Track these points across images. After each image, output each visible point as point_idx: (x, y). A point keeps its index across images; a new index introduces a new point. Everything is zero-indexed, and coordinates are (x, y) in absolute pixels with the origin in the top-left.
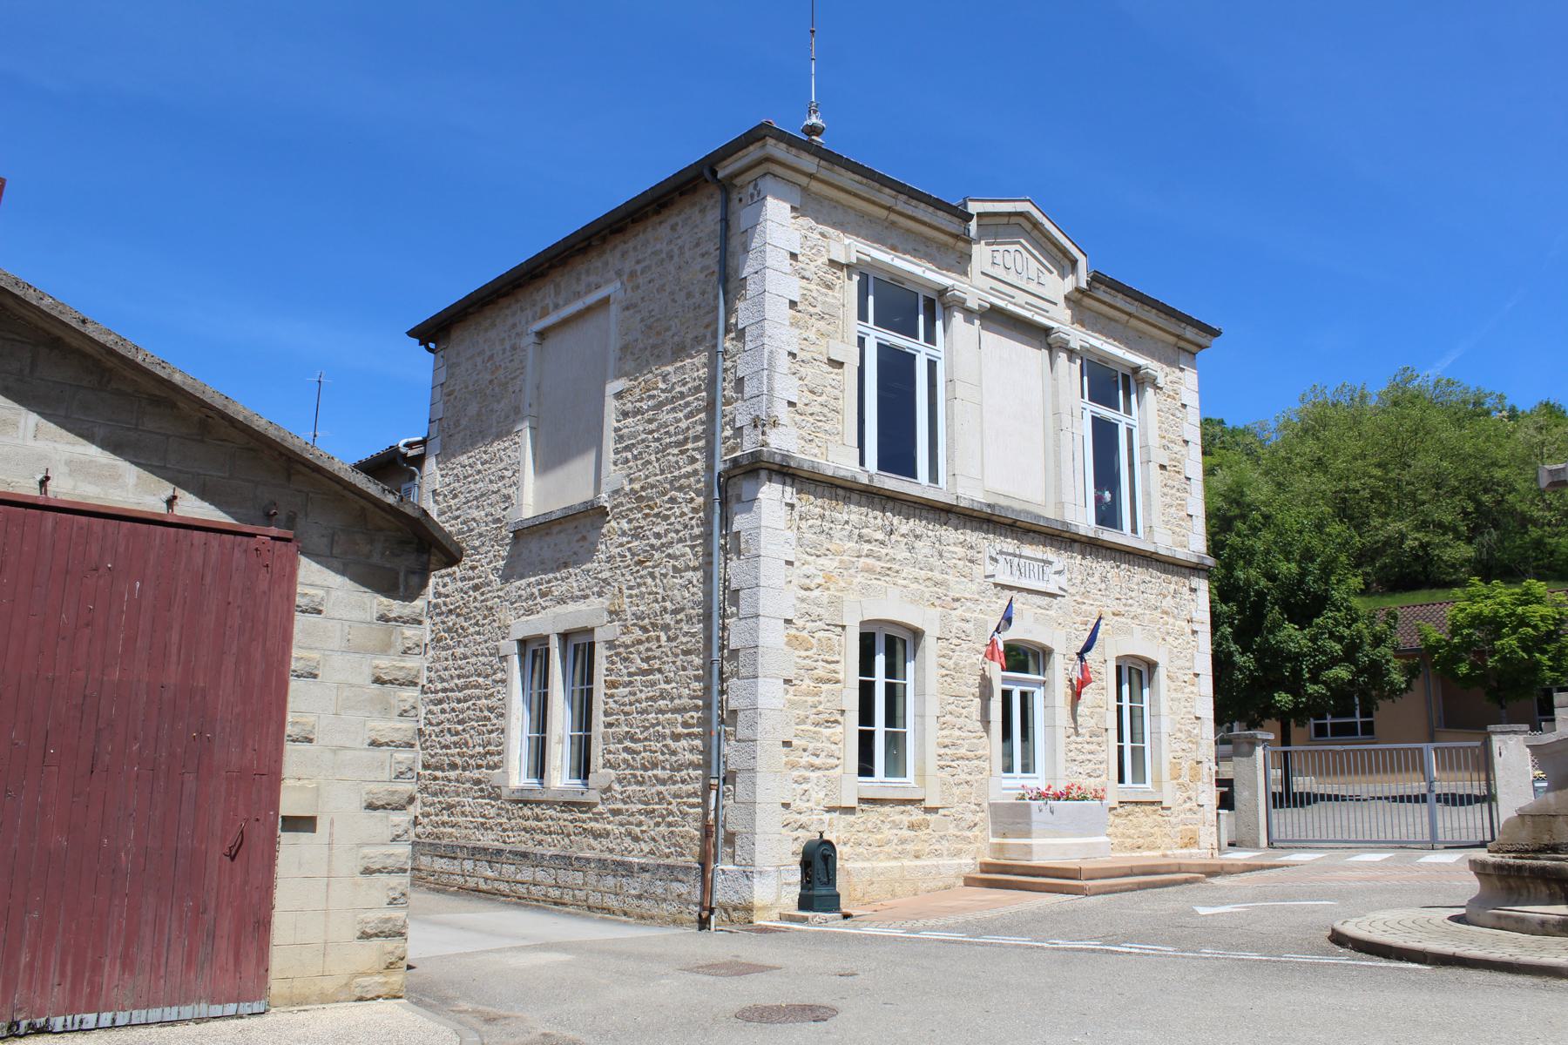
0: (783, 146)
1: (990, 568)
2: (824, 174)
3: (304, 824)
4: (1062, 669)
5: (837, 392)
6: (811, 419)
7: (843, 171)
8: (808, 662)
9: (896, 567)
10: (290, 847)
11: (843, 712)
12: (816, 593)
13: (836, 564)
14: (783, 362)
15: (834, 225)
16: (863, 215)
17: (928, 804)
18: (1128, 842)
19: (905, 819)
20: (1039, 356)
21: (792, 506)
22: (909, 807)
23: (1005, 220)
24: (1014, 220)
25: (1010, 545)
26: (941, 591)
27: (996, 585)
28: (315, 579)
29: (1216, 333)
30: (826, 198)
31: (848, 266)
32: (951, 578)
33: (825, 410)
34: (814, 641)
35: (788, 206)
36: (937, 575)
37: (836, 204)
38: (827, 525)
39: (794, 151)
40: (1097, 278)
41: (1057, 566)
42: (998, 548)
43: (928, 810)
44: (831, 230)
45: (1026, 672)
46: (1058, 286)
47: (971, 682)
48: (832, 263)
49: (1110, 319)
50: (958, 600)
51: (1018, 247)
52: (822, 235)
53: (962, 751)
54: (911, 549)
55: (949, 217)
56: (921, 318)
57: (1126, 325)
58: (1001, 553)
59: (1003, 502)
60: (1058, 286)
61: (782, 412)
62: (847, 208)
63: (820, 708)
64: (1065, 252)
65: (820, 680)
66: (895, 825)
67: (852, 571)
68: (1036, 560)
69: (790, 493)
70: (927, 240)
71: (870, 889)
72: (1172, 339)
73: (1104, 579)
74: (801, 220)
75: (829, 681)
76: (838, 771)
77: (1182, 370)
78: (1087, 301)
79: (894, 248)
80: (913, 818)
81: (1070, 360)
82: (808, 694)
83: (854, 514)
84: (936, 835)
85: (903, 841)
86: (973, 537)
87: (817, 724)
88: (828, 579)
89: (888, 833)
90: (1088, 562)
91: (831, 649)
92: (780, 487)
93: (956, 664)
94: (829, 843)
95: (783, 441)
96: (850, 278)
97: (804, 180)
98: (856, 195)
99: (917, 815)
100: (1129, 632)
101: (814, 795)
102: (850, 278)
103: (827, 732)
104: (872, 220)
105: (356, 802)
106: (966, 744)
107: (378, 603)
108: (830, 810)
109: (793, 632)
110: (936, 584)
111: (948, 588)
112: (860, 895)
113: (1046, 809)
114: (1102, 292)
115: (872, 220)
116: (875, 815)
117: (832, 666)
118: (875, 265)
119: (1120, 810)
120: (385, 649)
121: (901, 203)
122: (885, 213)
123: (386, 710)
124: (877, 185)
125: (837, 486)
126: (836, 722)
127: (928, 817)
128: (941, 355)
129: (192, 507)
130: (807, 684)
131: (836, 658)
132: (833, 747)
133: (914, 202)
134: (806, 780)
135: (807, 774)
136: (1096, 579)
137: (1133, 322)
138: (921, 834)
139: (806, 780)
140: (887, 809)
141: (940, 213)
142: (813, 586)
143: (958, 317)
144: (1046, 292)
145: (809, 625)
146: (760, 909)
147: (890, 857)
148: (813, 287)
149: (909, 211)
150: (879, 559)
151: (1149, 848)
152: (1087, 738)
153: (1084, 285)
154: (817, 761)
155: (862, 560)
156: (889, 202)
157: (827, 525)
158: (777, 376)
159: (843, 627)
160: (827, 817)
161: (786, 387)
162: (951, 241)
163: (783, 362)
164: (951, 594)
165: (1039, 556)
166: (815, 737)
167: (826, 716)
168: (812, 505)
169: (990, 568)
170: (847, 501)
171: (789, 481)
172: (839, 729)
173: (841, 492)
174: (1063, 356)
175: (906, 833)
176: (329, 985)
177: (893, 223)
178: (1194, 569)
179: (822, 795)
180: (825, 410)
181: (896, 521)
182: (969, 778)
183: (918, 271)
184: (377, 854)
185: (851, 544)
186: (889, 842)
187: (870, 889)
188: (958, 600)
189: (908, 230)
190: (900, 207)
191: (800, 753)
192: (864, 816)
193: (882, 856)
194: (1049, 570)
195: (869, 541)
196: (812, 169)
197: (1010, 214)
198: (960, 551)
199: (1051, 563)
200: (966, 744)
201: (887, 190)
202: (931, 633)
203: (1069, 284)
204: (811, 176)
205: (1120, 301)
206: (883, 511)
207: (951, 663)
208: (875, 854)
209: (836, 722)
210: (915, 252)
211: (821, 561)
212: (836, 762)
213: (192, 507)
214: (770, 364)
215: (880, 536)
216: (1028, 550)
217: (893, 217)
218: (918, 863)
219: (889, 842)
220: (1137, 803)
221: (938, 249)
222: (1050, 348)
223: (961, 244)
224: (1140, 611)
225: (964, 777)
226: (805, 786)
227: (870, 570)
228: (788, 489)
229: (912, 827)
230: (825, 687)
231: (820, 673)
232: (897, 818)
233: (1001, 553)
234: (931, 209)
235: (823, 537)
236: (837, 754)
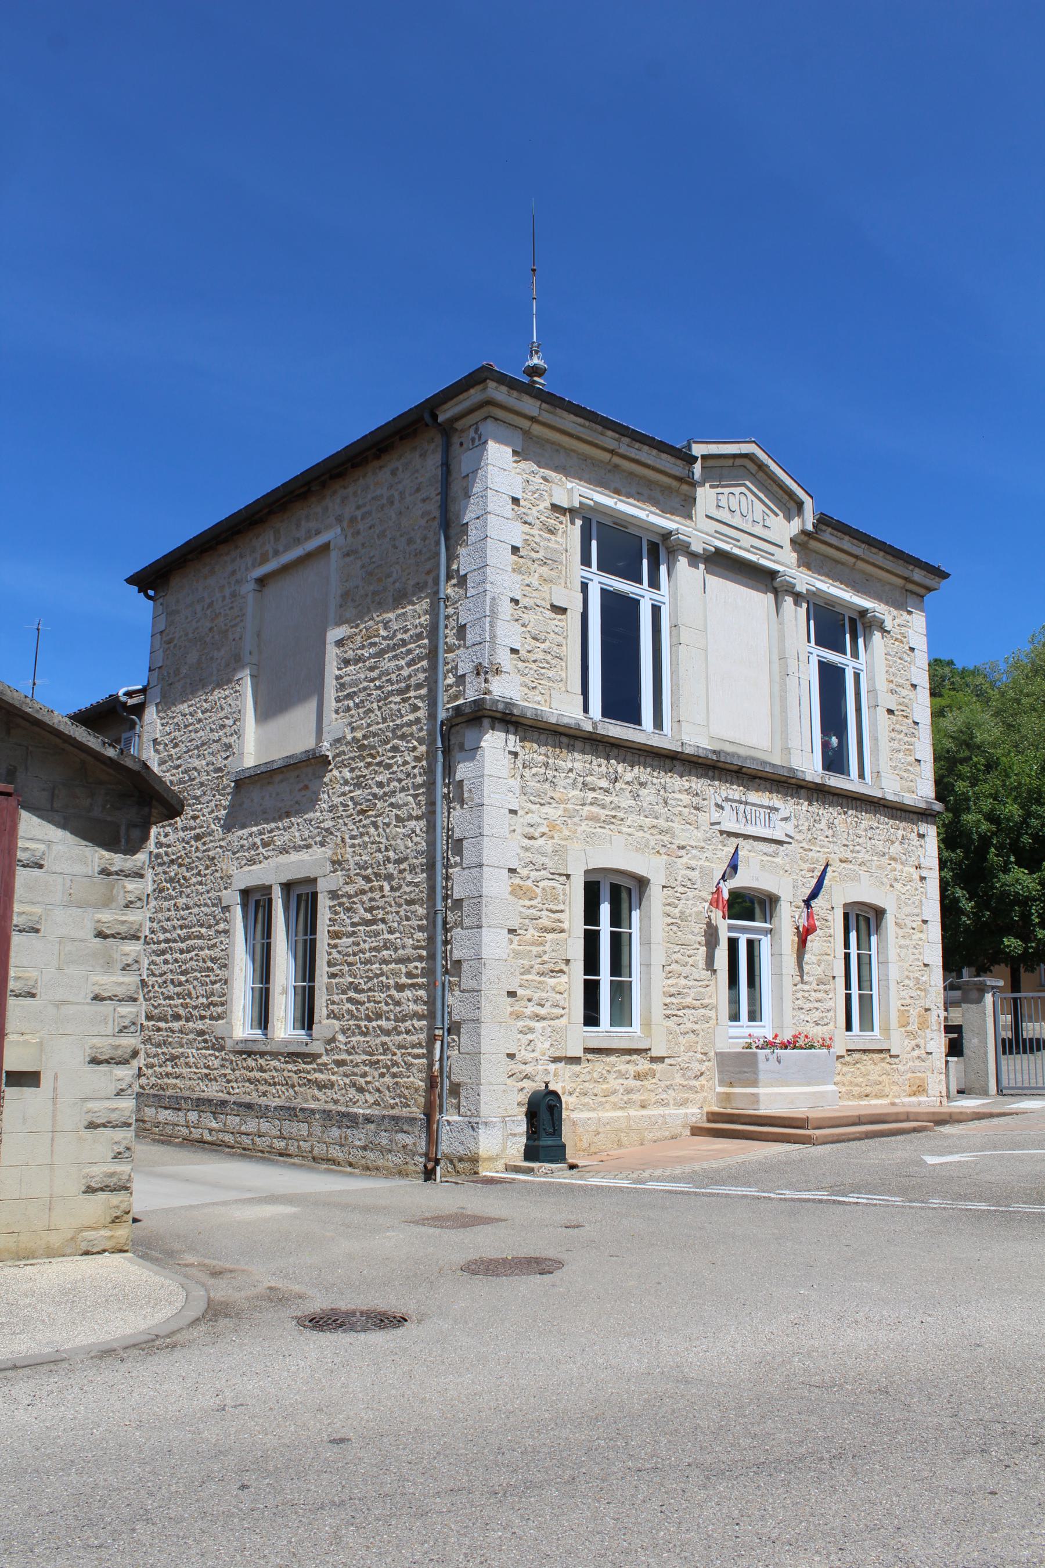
0: (504, 389)
1: (715, 816)
2: (546, 417)
3: (28, 1079)
4: (788, 917)
5: (560, 639)
6: (534, 666)
7: (565, 414)
9: (621, 815)
11: (568, 962)
12: (541, 842)
13: (560, 812)
14: (506, 609)
15: (556, 469)
16: (585, 458)
17: (654, 1053)
18: (856, 1090)
19: (631, 1068)
20: (762, 601)
21: (515, 755)
22: (635, 1057)
23: (730, 462)
25: (735, 792)
26: (666, 839)
27: (722, 832)
28: (34, 832)
29: (944, 575)
30: (548, 441)
31: (571, 510)
32: (676, 826)
33: (549, 657)
34: (538, 891)
35: (510, 450)
36: (662, 823)
37: (558, 447)
38: (550, 773)
39: (515, 394)
40: (823, 521)
41: (784, 813)
42: (724, 794)
43: (654, 1060)
44: (553, 474)
45: (753, 919)
46: (784, 529)
47: (697, 930)
48: (555, 507)
49: (837, 562)
50: (683, 848)
51: (743, 489)
52: (545, 479)
53: (689, 1000)
54: (636, 797)
55: (672, 460)
56: (645, 562)
57: (853, 568)
58: (727, 799)
59: (729, 748)
60: (784, 529)
61: (504, 659)
62: (569, 451)
63: (545, 958)
64: (791, 494)
65: (545, 930)
66: (621, 1075)
67: (576, 820)
68: (763, 807)
69: (513, 741)
70: (650, 483)
71: (595, 1139)
72: (900, 582)
73: (831, 825)
74: (524, 465)
75: (553, 930)
76: (563, 1021)
77: (910, 613)
78: (813, 544)
79: (617, 492)
80: (640, 1068)
81: (797, 603)
82: (533, 944)
83: (578, 761)
84: (663, 1084)
85: (629, 1091)
86: (698, 784)
87: (542, 974)
88: (552, 827)
89: (614, 1083)
90: (815, 808)
91: (556, 898)
92: (503, 735)
93: (682, 912)
94: (555, 1093)
95: (507, 688)
96: (573, 523)
97: (525, 424)
98: (579, 439)
99: (643, 1064)
100: (857, 878)
101: (539, 1045)
102: (573, 523)
103: (552, 982)
104: (595, 463)
105: (78, 1058)
106: (692, 993)
107: (99, 856)
108: (556, 1060)
109: (517, 881)
110: (661, 832)
111: (673, 836)
112: (585, 1145)
113: (773, 1059)
114: (828, 535)
115: (595, 463)
116: (600, 1065)
117: (557, 916)
118: (598, 509)
119: (847, 1059)
120: (107, 903)
121: (624, 446)
122: (606, 456)
123: (108, 964)
124: (600, 428)
125: (561, 734)
126: (561, 971)
127: (654, 1066)
128: (666, 600)
130: (532, 933)
131: (561, 907)
132: (558, 996)
133: (637, 445)
134: (531, 1030)
135: (532, 1024)
136: (823, 825)
137: (861, 565)
139: (531, 1030)
140: (612, 1059)
141: (664, 456)
142: (537, 835)
143: (683, 562)
144: (771, 535)
145: (533, 874)
146: (486, 1159)
147: (616, 1107)
148: (535, 532)
149: (633, 453)
150: (603, 807)
151: (877, 1097)
152: (814, 986)
153: (810, 527)
154: (542, 1011)
155: (587, 808)
156: (612, 444)
157: (550, 773)
158: (499, 623)
159: (568, 876)
160: (552, 1067)
161: (508, 634)
162: (675, 484)
163: (506, 609)
164: (677, 842)
165: (766, 803)
166: (540, 987)
167: (550, 966)
168: (535, 753)
169: (715, 816)
170: (571, 748)
171: (512, 729)
172: (564, 978)
173: (565, 740)
174: (789, 600)
175: (632, 1083)
176: (55, 1240)
177: (616, 466)
179: (547, 1045)
180: (549, 657)
181: (620, 768)
182: (695, 1027)
183: (642, 514)
184: (100, 1109)
185: (576, 792)
186: (615, 1092)
187: (595, 1139)
188: (683, 848)
190: (623, 449)
191: (525, 1003)
192: (590, 1064)
193: (607, 1106)
194: (776, 817)
195: (593, 789)
196: (534, 412)
197: (735, 456)
198: (685, 798)
199: (777, 810)
200: (692, 993)
201: (610, 433)
202: (657, 880)
203: (794, 527)
204: (533, 419)
205: (847, 543)
207: (676, 912)
208: (601, 1104)
209: (561, 971)
210: (639, 496)
211: (546, 809)
212: (562, 1012)
214: (492, 611)
215: (604, 783)
216: (754, 797)
217: (616, 460)
218: (644, 1112)
219: (615, 1092)
220: (864, 1051)
221: (662, 492)
222: (776, 592)
224: (867, 857)
225: (690, 1026)
226: (530, 1037)
227: (595, 818)
228: (511, 737)
229: (638, 1076)
230: (550, 936)
231: (545, 922)
232: (623, 1067)
233: (727, 799)
234: (655, 452)
235: (547, 785)
236: (561, 1004)
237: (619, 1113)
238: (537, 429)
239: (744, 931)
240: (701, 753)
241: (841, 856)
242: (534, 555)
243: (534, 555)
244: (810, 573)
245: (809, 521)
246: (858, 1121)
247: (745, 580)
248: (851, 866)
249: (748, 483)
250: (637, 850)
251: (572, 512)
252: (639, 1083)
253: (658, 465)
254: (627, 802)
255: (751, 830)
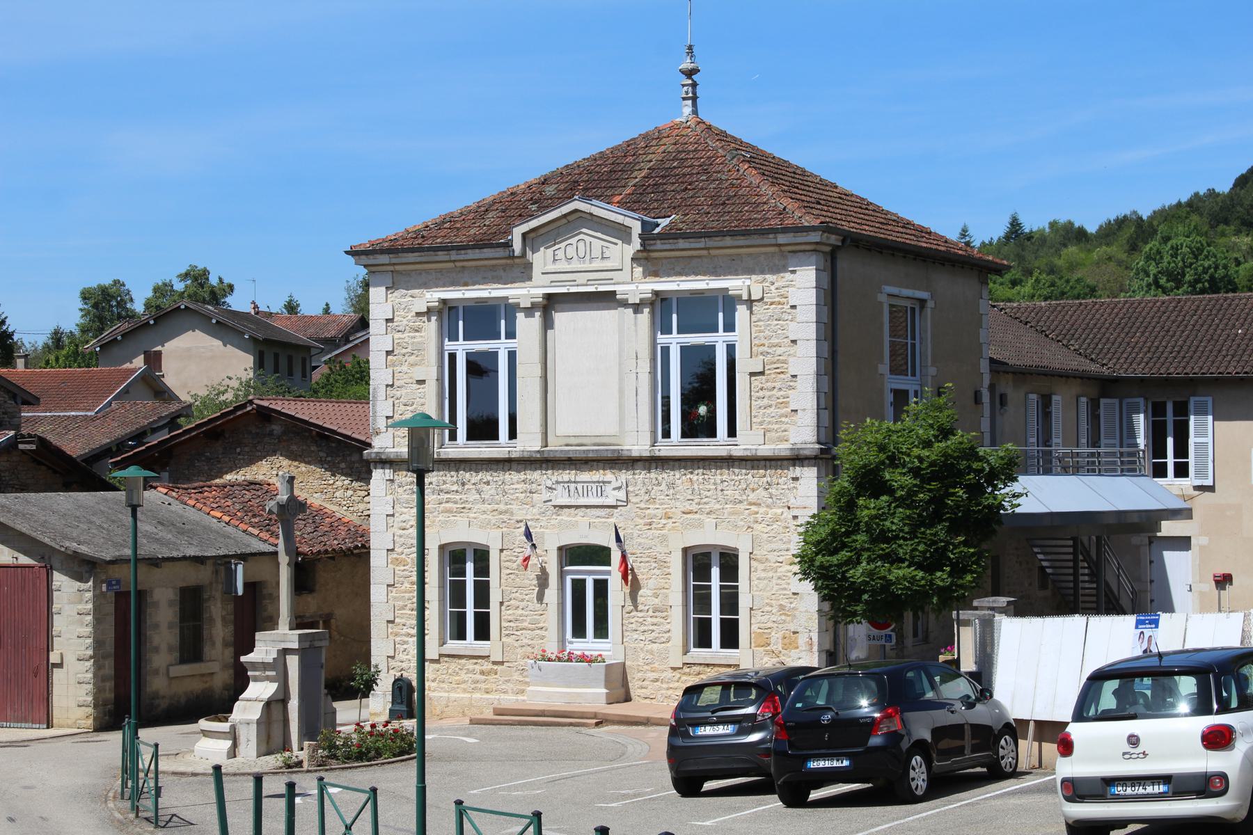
1: (546, 495)
2: (394, 261)
3: (60, 665)
8: (406, 573)
10: (57, 674)
16: (441, 271)
17: (492, 659)
19: (478, 667)
21: (392, 481)
23: (564, 221)
24: (570, 218)
25: (567, 475)
26: (505, 517)
27: (555, 507)
28: (59, 579)
36: (502, 507)
37: (420, 272)
42: (554, 479)
43: (494, 663)
44: (416, 291)
46: (622, 253)
48: (418, 314)
51: (581, 236)
53: (525, 624)
58: (558, 482)
61: (381, 423)
66: (468, 671)
69: (388, 473)
70: (493, 268)
72: (776, 249)
73: (671, 485)
77: (793, 272)
79: (466, 284)
80: (484, 668)
86: (536, 475)
97: (391, 268)
99: (487, 666)
100: (700, 525)
102: (429, 320)
105: (74, 659)
110: (501, 513)
111: (512, 514)
112: (438, 712)
113: (536, 667)
114: (659, 245)
116: (454, 665)
119: (686, 670)
120: (80, 602)
121: (454, 255)
122: (451, 265)
127: (495, 667)
129: (24, 560)
136: (663, 487)
137: (713, 252)
138: (492, 678)
140: (463, 661)
147: (465, 691)
148: (406, 335)
149: (461, 257)
150: (456, 503)
152: (650, 613)
153: (639, 247)
156: (447, 258)
169: (546, 495)
175: (479, 677)
176: (70, 722)
178: (797, 459)
181: (468, 475)
186: (465, 682)
189: (476, 267)
194: (608, 488)
197: (565, 216)
205: (682, 244)
206: (457, 471)
207: (515, 566)
210: (485, 281)
213: (24, 560)
215: (455, 488)
216: (585, 476)
217: (458, 264)
219: (465, 682)
220: (708, 665)
223: (517, 261)
224: (718, 506)
228: (387, 471)
229: (482, 673)
232: (471, 667)
233: (558, 482)
237: (468, 695)
238: (398, 268)
239: (589, 574)
240: (526, 455)
241: (685, 509)
242: (404, 351)
243: (404, 351)
244: (657, 279)
245: (636, 244)
246: (542, 713)
247: (595, 305)
248: (697, 516)
249: (584, 230)
250: (481, 527)
251: (429, 312)
252: (484, 677)
253: (483, 256)
254: (473, 496)
255: (582, 501)
